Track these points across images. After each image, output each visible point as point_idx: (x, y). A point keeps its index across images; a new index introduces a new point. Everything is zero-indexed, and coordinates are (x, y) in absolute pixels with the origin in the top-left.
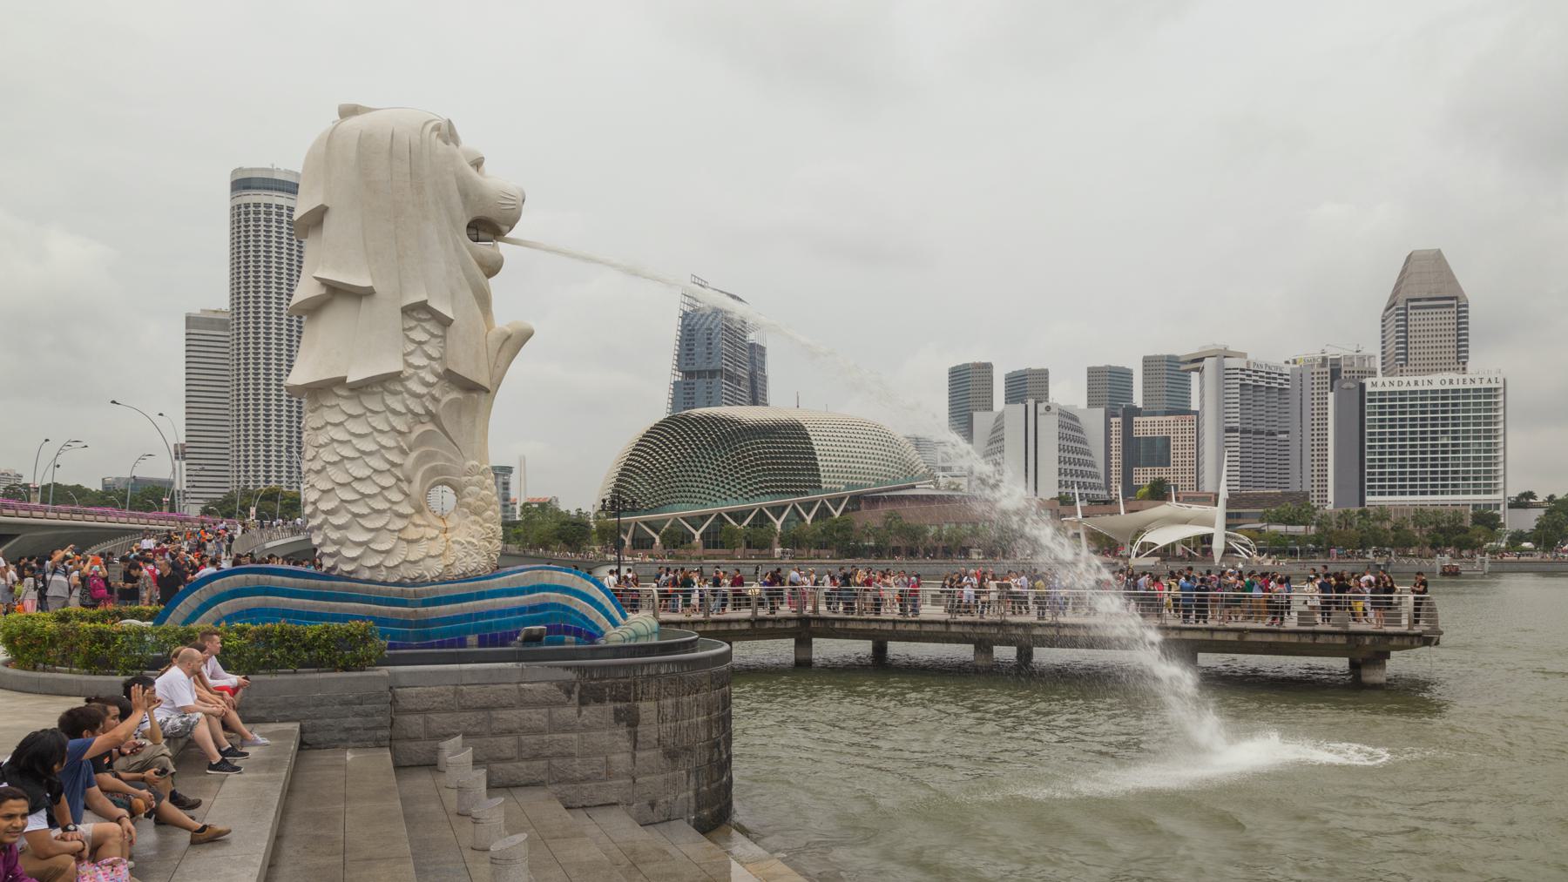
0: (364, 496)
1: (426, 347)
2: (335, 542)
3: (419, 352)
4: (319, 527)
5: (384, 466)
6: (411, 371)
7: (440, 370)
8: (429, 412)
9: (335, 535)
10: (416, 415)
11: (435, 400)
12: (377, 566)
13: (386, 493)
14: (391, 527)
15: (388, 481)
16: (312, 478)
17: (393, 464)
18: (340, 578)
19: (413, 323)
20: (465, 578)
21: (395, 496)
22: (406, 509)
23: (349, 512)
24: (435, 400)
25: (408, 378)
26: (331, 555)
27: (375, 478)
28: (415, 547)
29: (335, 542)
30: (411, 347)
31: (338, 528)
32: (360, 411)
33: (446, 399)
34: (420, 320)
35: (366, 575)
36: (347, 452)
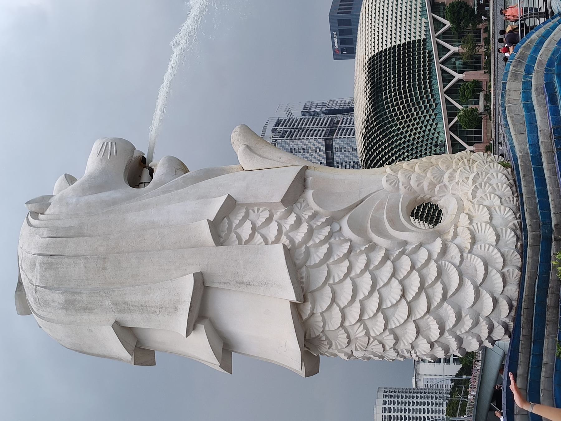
0: (422, 288)
1: (259, 223)
2: (476, 323)
3: (264, 231)
4: (460, 340)
5: (389, 265)
7: (282, 210)
8: (330, 222)
9: (468, 322)
10: (331, 234)
11: (315, 215)
12: (504, 276)
13: (419, 265)
14: (457, 261)
15: (405, 263)
16: (404, 346)
17: (386, 257)
18: (517, 320)
19: (233, 236)
20: (516, 186)
21: (423, 255)
22: (437, 246)
23: (440, 305)
24: (315, 215)
25: (292, 241)
26: (491, 329)
27: (402, 275)
29: (476, 323)
30: (258, 238)
31: (459, 318)
32: (328, 291)
33: (315, 207)
34: (230, 229)
36: (373, 305)
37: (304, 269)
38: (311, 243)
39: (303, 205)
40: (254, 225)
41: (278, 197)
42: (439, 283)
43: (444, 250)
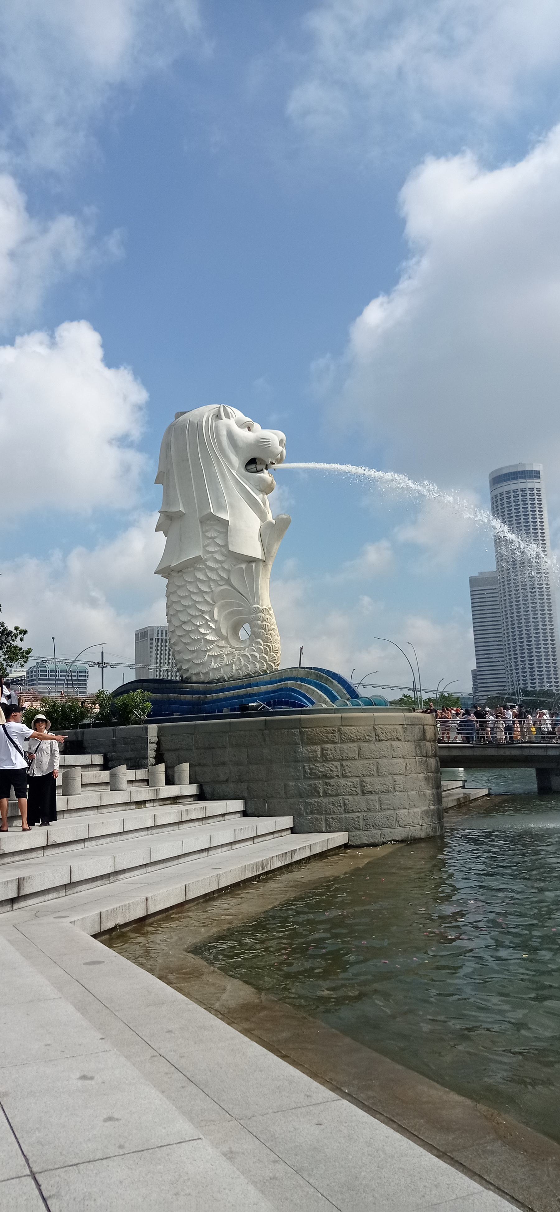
8: (222, 578)
25: (206, 560)
28: (218, 659)
30: (207, 542)
35: (194, 679)
37: (192, 569)
38: (207, 571)
40: (215, 537)
41: (231, 548)
43: (212, 642)
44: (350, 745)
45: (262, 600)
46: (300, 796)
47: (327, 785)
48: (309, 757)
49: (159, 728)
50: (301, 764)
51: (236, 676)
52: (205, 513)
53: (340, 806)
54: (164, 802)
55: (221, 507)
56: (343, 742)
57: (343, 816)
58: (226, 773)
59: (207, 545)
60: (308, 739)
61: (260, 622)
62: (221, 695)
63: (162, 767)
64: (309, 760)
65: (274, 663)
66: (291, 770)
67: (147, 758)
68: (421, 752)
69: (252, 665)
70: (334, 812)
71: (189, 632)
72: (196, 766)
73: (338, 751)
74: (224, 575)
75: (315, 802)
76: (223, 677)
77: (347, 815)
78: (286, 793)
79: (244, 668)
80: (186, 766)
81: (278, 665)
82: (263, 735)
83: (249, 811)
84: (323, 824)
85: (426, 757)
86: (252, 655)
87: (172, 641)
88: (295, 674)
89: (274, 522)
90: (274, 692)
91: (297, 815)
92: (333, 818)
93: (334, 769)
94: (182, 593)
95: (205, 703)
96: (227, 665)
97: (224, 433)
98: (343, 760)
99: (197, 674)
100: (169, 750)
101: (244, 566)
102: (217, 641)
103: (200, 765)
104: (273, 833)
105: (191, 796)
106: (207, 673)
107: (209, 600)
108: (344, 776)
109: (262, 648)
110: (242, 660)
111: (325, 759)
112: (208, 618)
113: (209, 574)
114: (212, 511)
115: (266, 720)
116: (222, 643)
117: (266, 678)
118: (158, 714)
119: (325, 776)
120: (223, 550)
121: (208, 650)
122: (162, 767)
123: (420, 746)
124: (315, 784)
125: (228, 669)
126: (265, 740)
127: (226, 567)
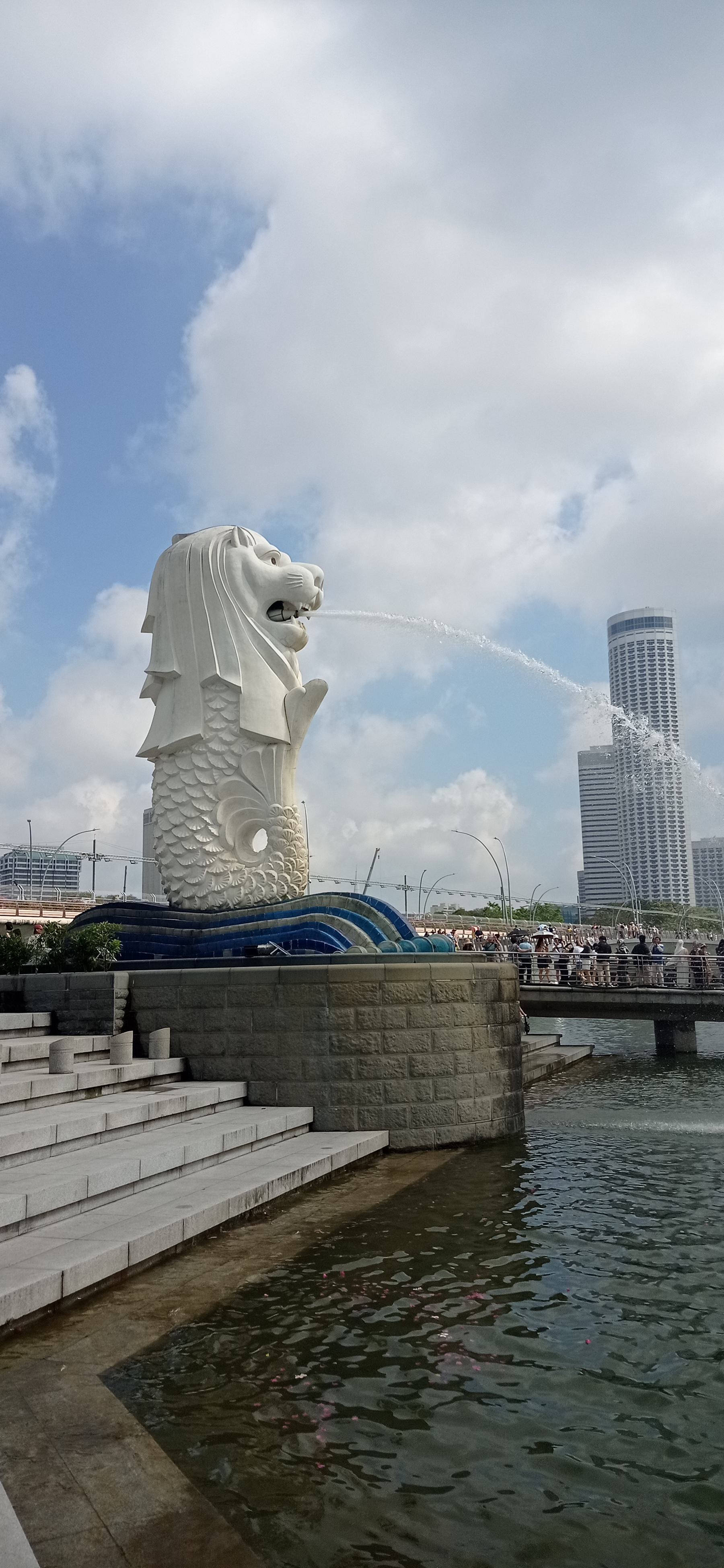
1: (223, 713)
6: (212, 734)
8: (230, 766)
25: (209, 741)
30: (211, 714)
35: (187, 905)
37: (189, 752)
38: (209, 755)
39: (247, 746)
40: (222, 709)
42: (184, 851)
43: (213, 854)
44: (396, 1008)
45: (285, 798)
46: (324, 1078)
47: (361, 1064)
48: (338, 1025)
49: (131, 977)
50: (327, 1034)
51: (245, 903)
52: (209, 675)
53: (380, 1094)
54: (130, 1087)
55: (231, 668)
56: (386, 1004)
57: (383, 1108)
58: (222, 1043)
59: (211, 720)
60: (337, 998)
61: (280, 828)
62: (222, 929)
63: (129, 1035)
64: (338, 1028)
65: (298, 886)
66: (313, 1042)
67: (112, 1020)
68: (495, 1017)
69: (267, 888)
70: (370, 1102)
71: (181, 839)
72: (181, 1032)
73: (379, 1017)
74: (233, 762)
75: (345, 1087)
76: (226, 904)
77: (389, 1107)
78: (304, 1074)
79: (256, 892)
80: (165, 1034)
81: (304, 888)
82: (275, 990)
83: (252, 1098)
84: (355, 1118)
85: (502, 1024)
86: (267, 874)
87: (159, 851)
88: (325, 902)
89: (304, 690)
90: (294, 927)
91: (318, 1106)
92: (368, 1111)
93: (373, 1042)
94: (173, 784)
95: (198, 941)
96: (233, 887)
97: (238, 565)
98: (385, 1029)
99: (191, 898)
100: (144, 1008)
101: (260, 750)
102: (220, 853)
103: (185, 1030)
104: (282, 1133)
105: (170, 1075)
106: (205, 897)
107: (211, 796)
108: (386, 1052)
109: (282, 864)
110: (254, 881)
111: (361, 1027)
112: (208, 821)
113: (213, 760)
114: (218, 673)
115: (279, 971)
116: (226, 856)
117: (286, 907)
118: (133, 954)
119: (360, 1052)
120: (233, 727)
121: (207, 866)
122: (129, 1035)
123: (493, 1009)
124: (345, 1063)
125: (234, 892)
126: (277, 999)
127: (236, 751)
